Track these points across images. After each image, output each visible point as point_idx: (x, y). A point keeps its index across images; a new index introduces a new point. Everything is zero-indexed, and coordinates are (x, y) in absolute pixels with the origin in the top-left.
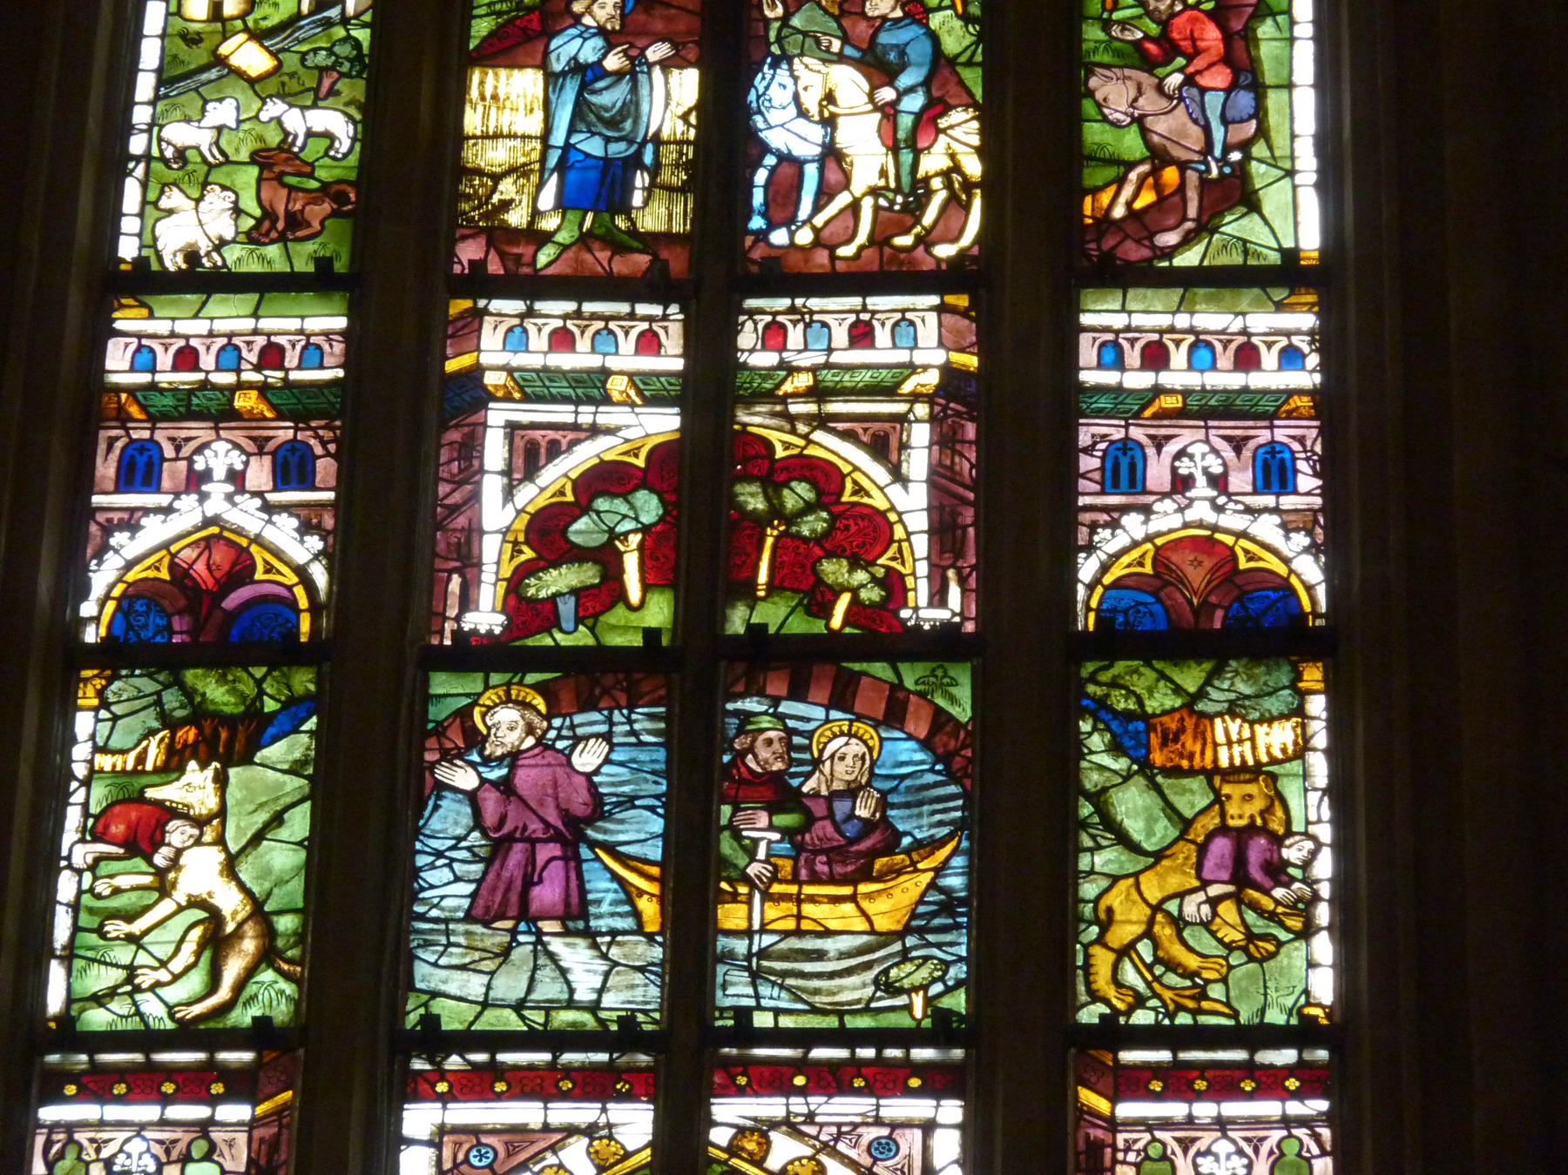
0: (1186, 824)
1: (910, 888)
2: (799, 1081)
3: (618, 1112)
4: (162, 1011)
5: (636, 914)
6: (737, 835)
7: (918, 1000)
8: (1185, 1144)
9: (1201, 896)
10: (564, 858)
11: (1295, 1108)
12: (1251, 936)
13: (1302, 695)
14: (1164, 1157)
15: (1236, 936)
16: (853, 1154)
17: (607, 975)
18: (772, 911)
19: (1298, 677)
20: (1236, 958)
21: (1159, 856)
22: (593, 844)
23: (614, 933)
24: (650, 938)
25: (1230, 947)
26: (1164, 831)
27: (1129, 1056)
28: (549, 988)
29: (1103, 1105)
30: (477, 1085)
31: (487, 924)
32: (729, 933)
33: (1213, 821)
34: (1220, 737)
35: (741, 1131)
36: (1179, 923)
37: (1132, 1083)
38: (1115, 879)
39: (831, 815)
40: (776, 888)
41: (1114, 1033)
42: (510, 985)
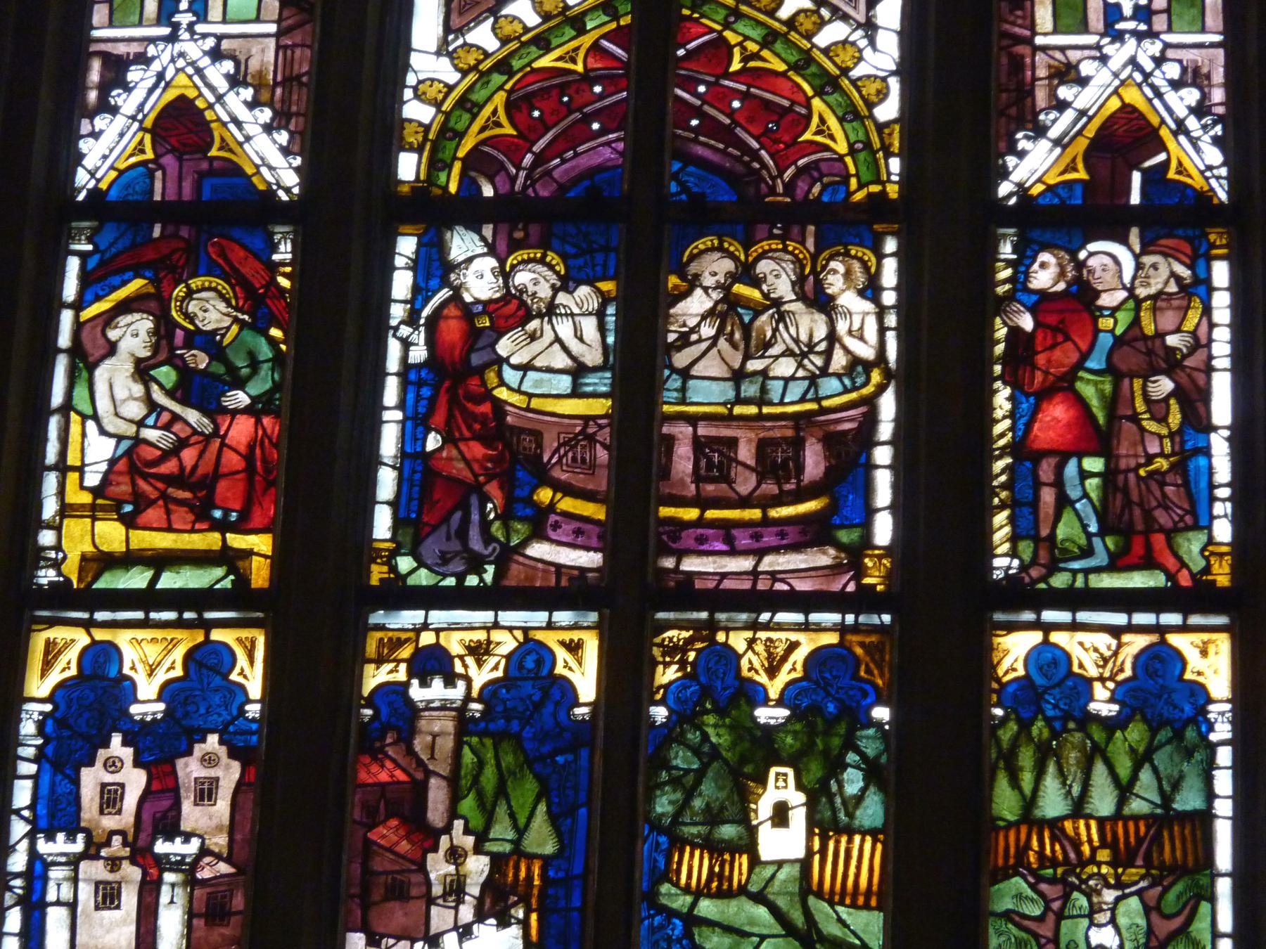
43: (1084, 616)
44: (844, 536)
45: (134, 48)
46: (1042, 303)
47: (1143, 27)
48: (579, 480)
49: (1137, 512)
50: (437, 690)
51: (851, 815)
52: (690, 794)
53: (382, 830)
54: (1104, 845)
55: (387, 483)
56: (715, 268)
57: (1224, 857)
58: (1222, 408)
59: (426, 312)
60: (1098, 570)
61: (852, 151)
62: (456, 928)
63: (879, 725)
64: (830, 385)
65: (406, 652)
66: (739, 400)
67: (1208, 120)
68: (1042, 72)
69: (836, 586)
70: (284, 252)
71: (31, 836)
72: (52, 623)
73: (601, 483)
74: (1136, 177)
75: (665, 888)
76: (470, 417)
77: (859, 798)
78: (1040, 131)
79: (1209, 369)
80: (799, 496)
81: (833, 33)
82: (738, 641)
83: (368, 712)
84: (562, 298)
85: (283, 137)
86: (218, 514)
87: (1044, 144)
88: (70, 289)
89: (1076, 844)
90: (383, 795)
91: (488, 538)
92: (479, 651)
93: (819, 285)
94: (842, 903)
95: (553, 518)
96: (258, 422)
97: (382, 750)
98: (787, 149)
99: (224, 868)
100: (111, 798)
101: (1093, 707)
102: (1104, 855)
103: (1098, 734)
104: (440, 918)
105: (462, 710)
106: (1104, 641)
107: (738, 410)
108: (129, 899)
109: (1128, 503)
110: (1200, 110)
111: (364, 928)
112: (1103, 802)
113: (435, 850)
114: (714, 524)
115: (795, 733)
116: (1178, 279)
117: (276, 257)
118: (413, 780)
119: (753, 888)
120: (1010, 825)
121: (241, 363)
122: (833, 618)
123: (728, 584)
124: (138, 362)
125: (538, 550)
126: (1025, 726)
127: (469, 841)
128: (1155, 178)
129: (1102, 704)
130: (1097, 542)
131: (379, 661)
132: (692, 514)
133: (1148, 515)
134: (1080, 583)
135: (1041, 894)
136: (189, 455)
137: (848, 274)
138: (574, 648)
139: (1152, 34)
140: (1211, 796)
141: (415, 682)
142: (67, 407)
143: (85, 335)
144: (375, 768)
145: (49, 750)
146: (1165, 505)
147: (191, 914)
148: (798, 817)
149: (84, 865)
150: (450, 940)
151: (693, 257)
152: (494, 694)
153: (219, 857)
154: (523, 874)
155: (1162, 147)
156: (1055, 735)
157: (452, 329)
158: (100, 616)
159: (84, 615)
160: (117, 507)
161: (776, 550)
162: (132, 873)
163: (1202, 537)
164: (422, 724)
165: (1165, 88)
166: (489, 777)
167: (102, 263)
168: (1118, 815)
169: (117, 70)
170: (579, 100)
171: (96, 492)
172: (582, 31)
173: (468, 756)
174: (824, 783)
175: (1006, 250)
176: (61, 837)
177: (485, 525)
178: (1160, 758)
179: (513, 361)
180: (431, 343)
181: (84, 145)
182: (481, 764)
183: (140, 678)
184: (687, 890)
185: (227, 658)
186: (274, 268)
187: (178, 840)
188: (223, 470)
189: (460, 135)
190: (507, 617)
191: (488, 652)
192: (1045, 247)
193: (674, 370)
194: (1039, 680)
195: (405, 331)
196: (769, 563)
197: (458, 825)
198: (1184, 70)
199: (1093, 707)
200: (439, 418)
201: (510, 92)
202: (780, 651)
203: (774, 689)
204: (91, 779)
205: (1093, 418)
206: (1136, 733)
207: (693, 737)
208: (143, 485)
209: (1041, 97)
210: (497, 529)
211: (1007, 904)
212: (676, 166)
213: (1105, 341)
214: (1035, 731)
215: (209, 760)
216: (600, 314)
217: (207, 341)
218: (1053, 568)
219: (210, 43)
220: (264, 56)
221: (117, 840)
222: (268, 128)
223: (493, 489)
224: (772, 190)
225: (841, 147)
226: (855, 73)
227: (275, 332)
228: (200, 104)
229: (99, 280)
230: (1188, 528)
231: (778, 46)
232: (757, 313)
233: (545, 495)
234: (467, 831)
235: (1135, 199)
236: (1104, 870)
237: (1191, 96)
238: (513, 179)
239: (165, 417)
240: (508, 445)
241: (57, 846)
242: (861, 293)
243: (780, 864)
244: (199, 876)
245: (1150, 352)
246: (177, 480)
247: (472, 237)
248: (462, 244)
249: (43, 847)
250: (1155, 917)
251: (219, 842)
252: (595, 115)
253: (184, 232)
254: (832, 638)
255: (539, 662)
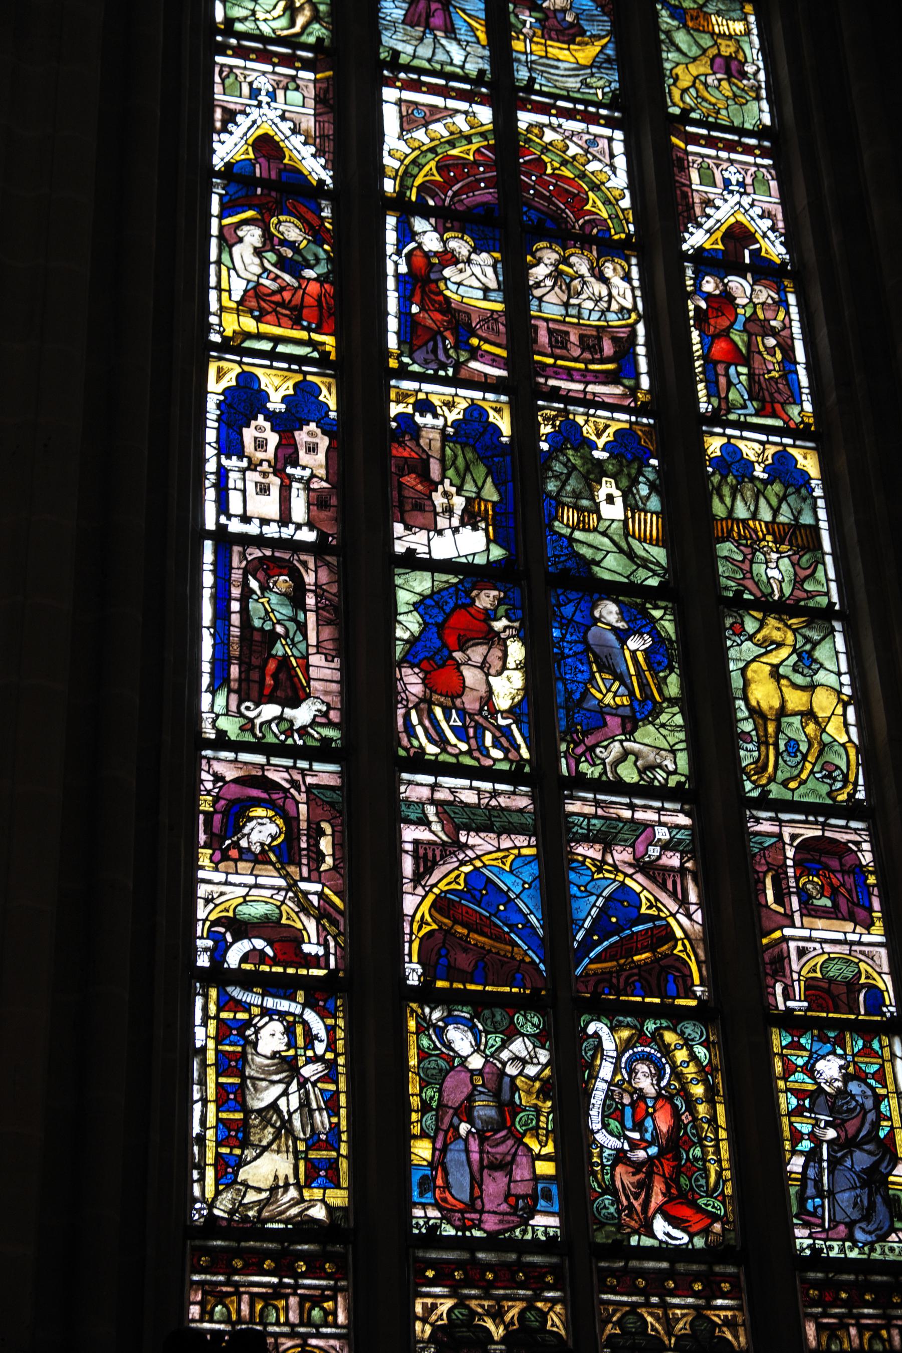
0: (704, 51)
1: (592, 51)
2: (554, 112)
3: (476, 108)
4: (270, 31)
5: (477, 38)
6: (517, 16)
7: (600, 92)
8: (718, 166)
9: (713, 77)
10: (443, 9)
11: (759, 161)
12: (735, 96)
13: (746, 14)
14: (708, 168)
15: (730, 94)
16: (580, 143)
17: (466, 57)
18: (534, 47)
19: (743, 7)
20: (730, 102)
21: (695, 59)
22: (455, 7)
23: (468, 42)
24: (484, 47)
25: (727, 98)
26: (694, 51)
27: (689, 129)
28: (441, 56)
29: (682, 145)
30: (415, 86)
31: (412, 27)
32: (517, 52)
33: (714, 51)
34: (714, 22)
35: (531, 125)
36: (706, 85)
37: (694, 139)
38: (678, 64)
39: (556, 17)
40: (535, 39)
41: (685, 117)
42: (425, 51)
43: (746, 434)
44: (626, 382)
45: (239, 107)
46: (708, 297)
47: (742, 190)
48: (492, 337)
49: (766, 393)
50: (428, 420)
51: (645, 504)
52: (564, 484)
53: (407, 478)
54: (768, 533)
55: (393, 324)
56: (550, 256)
57: (827, 546)
58: (800, 355)
59: (405, 251)
60: (751, 415)
61: (610, 217)
62: (450, 527)
63: (654, 467)
64: (611, 316)
65: (412, 400)
66: (567, 315)
67: (777, 234)
68: (697, 200)
69: (626, 403)
70: (326, 213)
71: (218, 456)
72: (220, 359)
73: (503, 340)
74: (747, 252)
75: (556, 523)
76: (433, 302)
77: (648, 497)
78: (699, 226)
79: (792, 339)
80: (602, 361)
81: (594, 166)
82: (580, 420)
83: (394, 424)
84: (473, 256)
85: (322, 161)
86: (305, 323)
87: (701, 232)
88: (215, 209)
89: (756, 532)
90: (406, 462)
91: (448, 357)
92: (450, 405)
93: (601, 273)
94: (645, 541)
95: (480, 352)
96: (322, 286)
97: (403, 442)
98: (580, 212)
99: (324, 484)
100: (260, 444)
101: (755, 473)
102: (769, 538)
103: (760, 486)
104: (442, 522)
105: (443, 430)
106: (757, 446)
107: (568, 319)
108: (275, 491)
109: (761, 388)
110: (773, 229)
111: (402, 521)
112: (766, 515)
113: (436, 491)
114: (561, 367)
115: (613, 465)
116: (772, 298)
117: (323, 214)
118: (421, 458)
119: (601, 529)
120: (722, 519)
121: (310, 257)
122: (625, 417)
123: (571, 394)
124: (255, 249)
125: (474, 365)
126: (724, 477)
127: (453, 490)
128: (756, 254)
129: (759, 472)
130: (748, 403)
131: (398, 402)
132: (550, 361)
133: (771, 394)
134: (742, 419)
135: (741, 551)
136: (287, 295)
137: (615, 270)
138: (498, 410)
139: (745, 193)
140: (817, 520)
141: (417, 414)
142: (219, 262)
143: (225, 230)
144: (401, 450)
145: (224, 417)
146: (778, 391)
147: (309, 504)
148: (619, 501)
149: (248, 473)
150: (448, 533)
151: (537, 250)
152: (459, 425)
153: (321, 479)
154: (483, 508)
155: (757, 242)
156: (739, 483)
157: (419, 259)
158: (245, 360)
159: (238, 359)
160: (251, 311)
161: (594, 383)
162: (275, 482)
163: (798, 409)
164: (423, 433)
165: (756, 217)
166: (460, 462)
167: (230, 200)
168: (774, 521)
169: (230, 116)
170: (473, 172)
171: (239, 303)
172: (470, 142)
173: (448, 451)
174: (629, 489)
175: (689, 273)
176: (234, 458)
177: (446, 351)
178: (791, 499)
179: (453, 280)
180: (408, 264)
181: (216, 146)
182: (456, 456)
183: (270, 390)
184: (567, 526)
185: (317, 391)
186: (323, 219)
187: (299, 468)
188: (305, 304)
189: (415, 177)
190: (462, 392)
191: (453, 406)
192: (708, 274)
193: (534, 297)
194: (728, 459)
195: (395, 258)
196: (591, 388)
197: (447, 482)
198: (763, 211)
199: (755, 473)
200: (417, 298)
201: (438, 162)
202: (601, 427)
203: (601, 443)
204: (249, 435)
205: (740, 351)
206: (777, 487)
207: (563, 458)
208: (263, 304)
209: (698, 211)
210: (451, 352)
211: (725, 553)
212: (525, 209)
213: (741, 319)
214: (729, 480)
215: (311, 434)
216: (494, 267)
217: (292, 245)
218: (729, 411)
219: (280, 112)
220: (308, 123)
221: (265, 464)
222: (314, 156)
223: (447, 334)
224: (574, 227)
225: (605, 215)
226: (607, 185)
227: (326, 247)
228: (276, 138)
229: (230, 208)
230: (790, 403)
231: (569, 166)
232: (572, 279)
233: (475, 341)
234: (452, 485)
235: (747, 261)
236: (771, 544)
237: (769, 223)
238: (444, 200)
239: (272, 276)
240: (454, 316)
241: (232, 463)
242: (622, 279)
243: (613, 521)
244: (312, 486)
245: (763, 327)
246: (283, 304)
247: (424, 222)
248: (419, 224)
249: (224, 461)
250: (797, 568)
251: (322, 472)
252: (483, 180)
253: (273, 194)
254: (627, 426)
255: (481, 415)
